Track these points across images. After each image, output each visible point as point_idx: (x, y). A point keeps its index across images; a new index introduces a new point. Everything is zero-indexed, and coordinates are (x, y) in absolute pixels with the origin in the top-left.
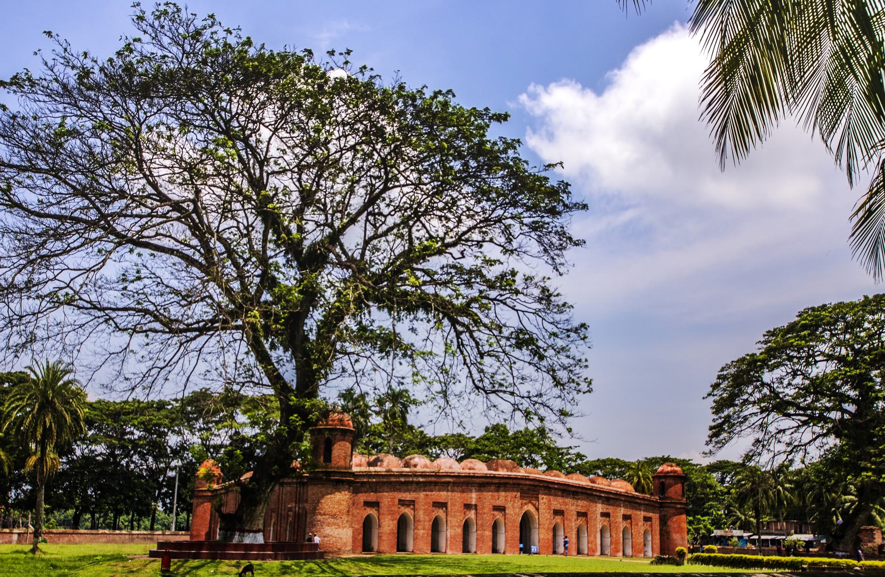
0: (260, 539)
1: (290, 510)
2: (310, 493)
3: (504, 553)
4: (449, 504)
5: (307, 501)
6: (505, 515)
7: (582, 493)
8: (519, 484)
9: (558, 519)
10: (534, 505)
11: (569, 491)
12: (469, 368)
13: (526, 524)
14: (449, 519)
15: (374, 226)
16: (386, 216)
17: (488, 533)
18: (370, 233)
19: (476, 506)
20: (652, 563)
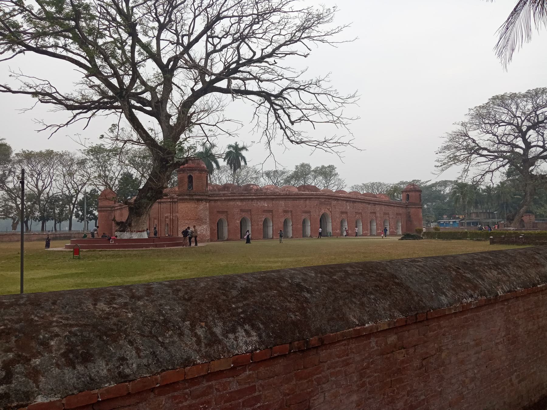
0: (145, 235)
1: (167, 217)
2: (179, 208)
3: (311, 236)
4: (274, 211)
5: (178, 212)
6: (310, 215)
7: (358, 202)
8: (319, 198)
9: (344, 216)
10: (329, 209)
11: (350, 201)
12: (284, 131)
13: (323, 220)
14: (274, 219)
15: (213, 45)
16: (220, 39)
17: (300, 226)
18: (210, 48)
19: (291, 211)
20: (402, 239)
